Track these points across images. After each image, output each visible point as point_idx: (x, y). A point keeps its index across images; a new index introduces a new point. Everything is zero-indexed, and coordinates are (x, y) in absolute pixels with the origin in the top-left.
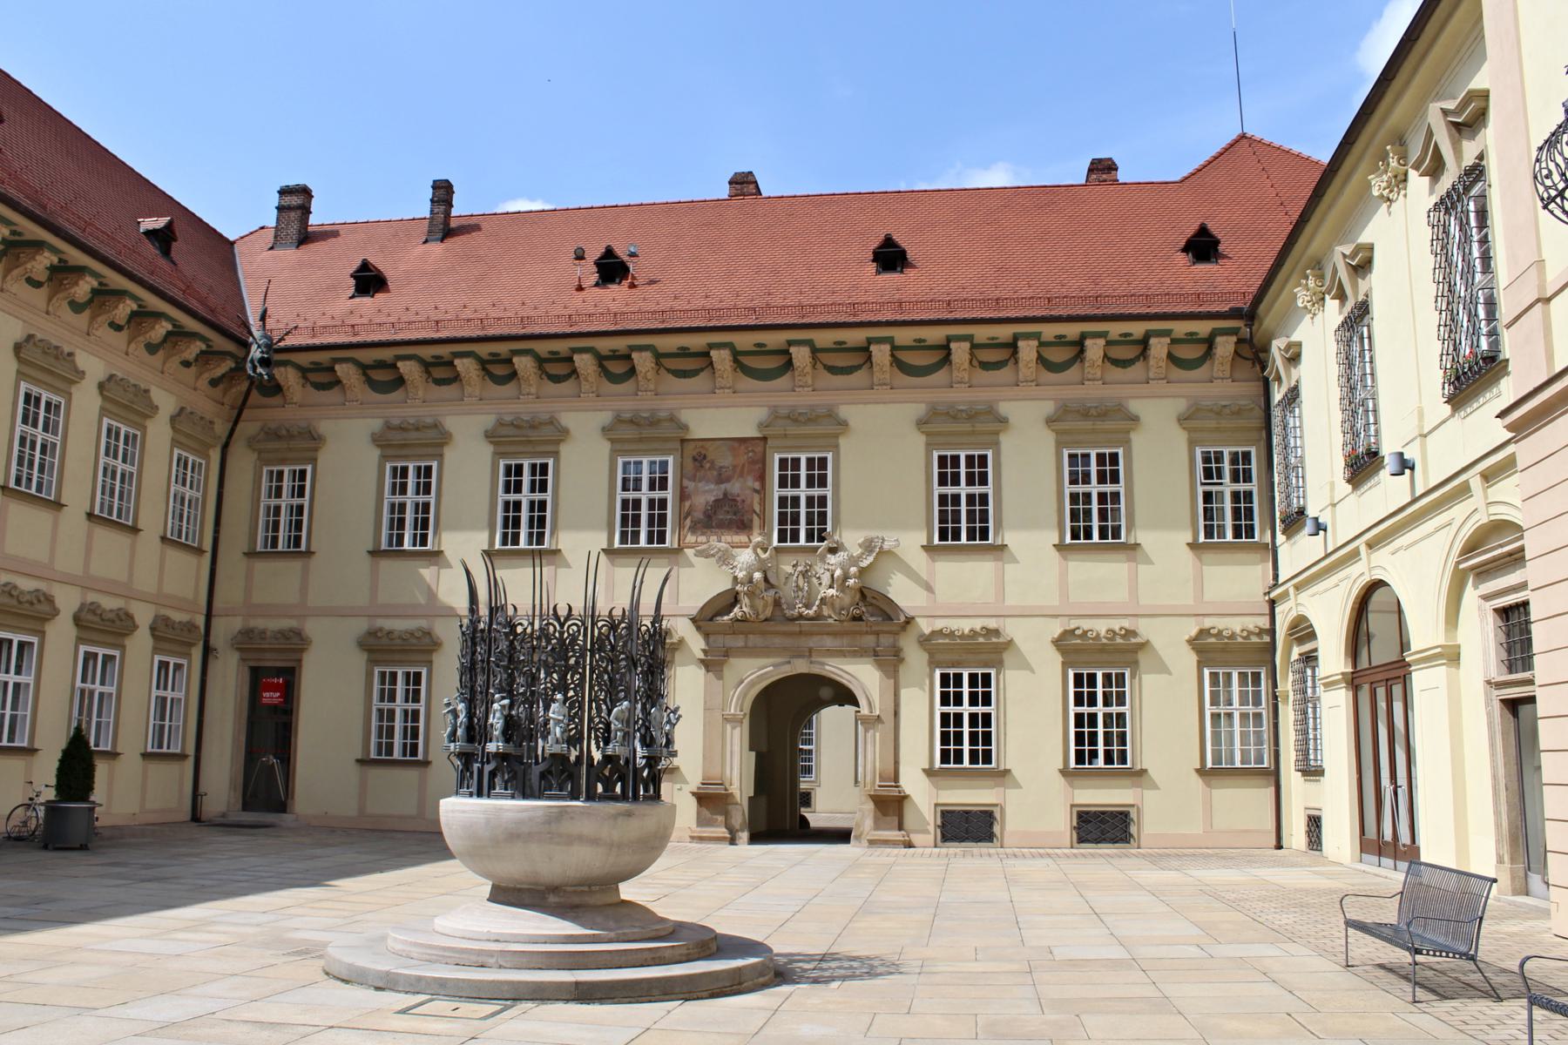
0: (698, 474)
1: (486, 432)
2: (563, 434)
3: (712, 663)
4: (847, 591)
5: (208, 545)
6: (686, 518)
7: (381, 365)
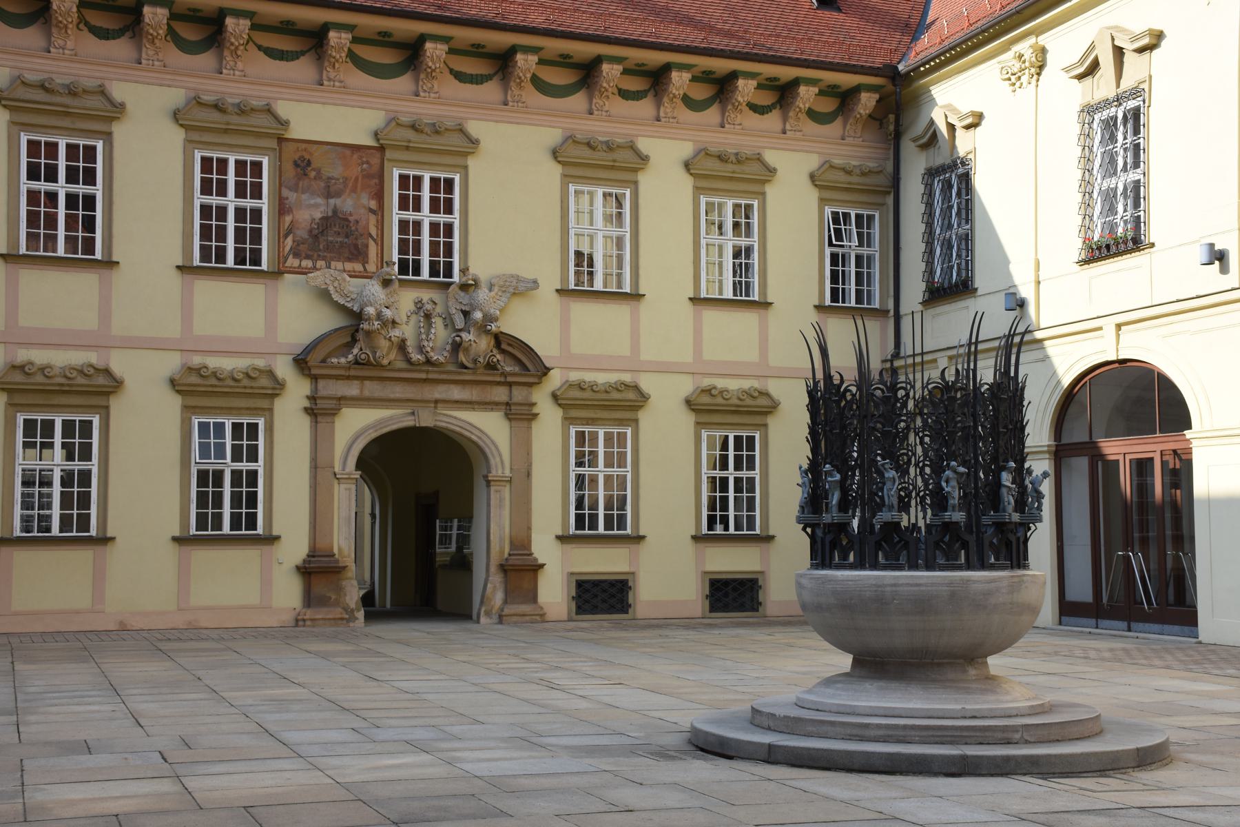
0: (301, 185)
2: (117, 110)
6: (286, 236)
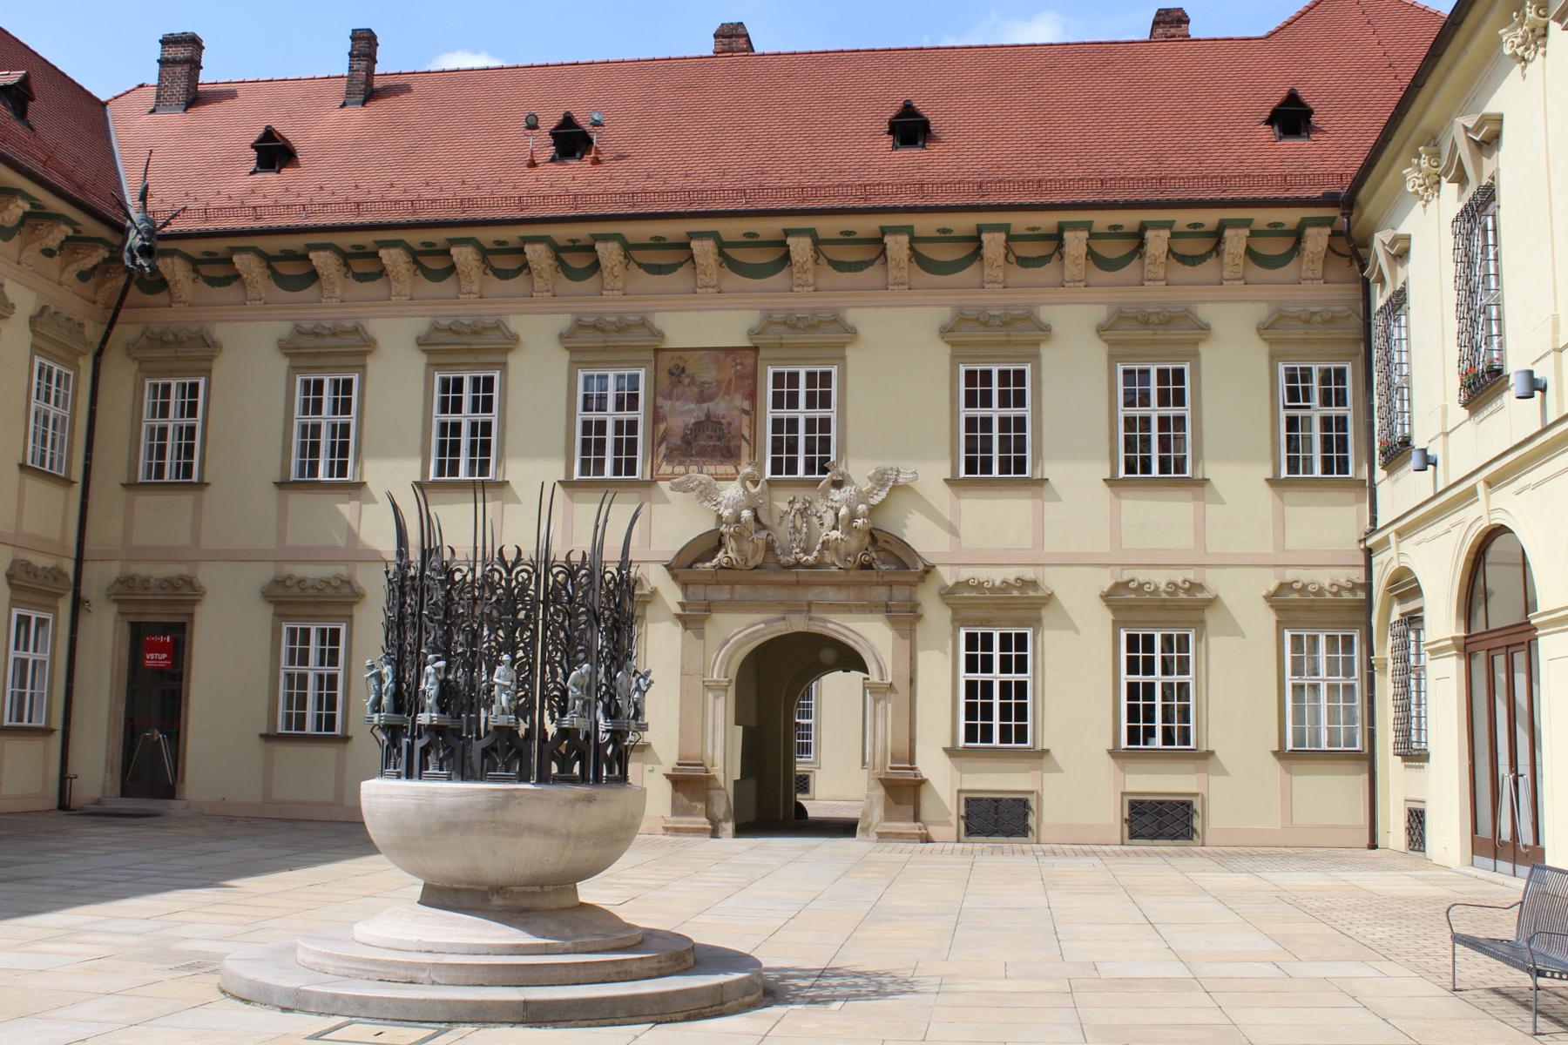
0: (675, 392)
1: (418, 338)
3: (692, 619)
4: (854, 533)
5: (77, 474)
6: (660, 445)
7: (289, 256)
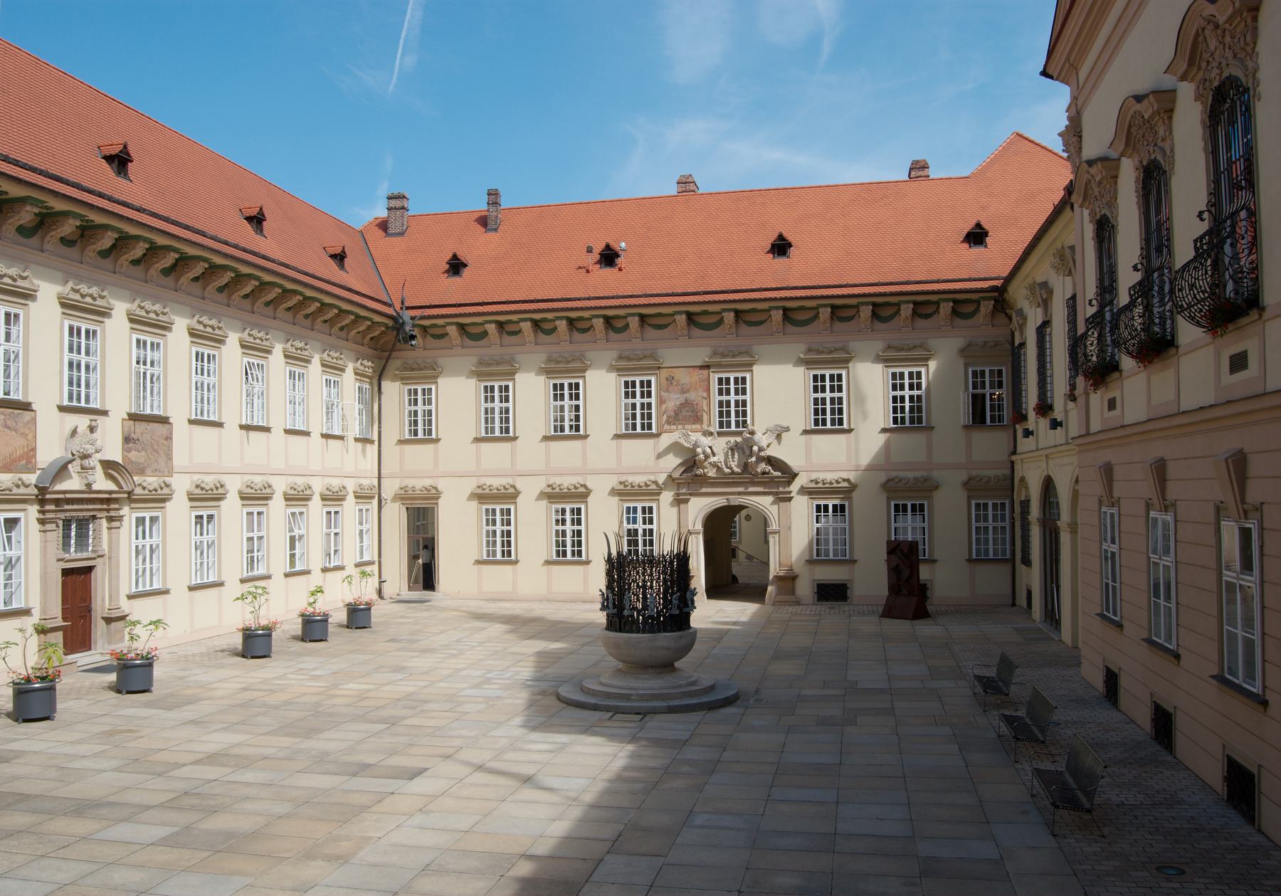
3: (679, 501)
5: (376, 438)
